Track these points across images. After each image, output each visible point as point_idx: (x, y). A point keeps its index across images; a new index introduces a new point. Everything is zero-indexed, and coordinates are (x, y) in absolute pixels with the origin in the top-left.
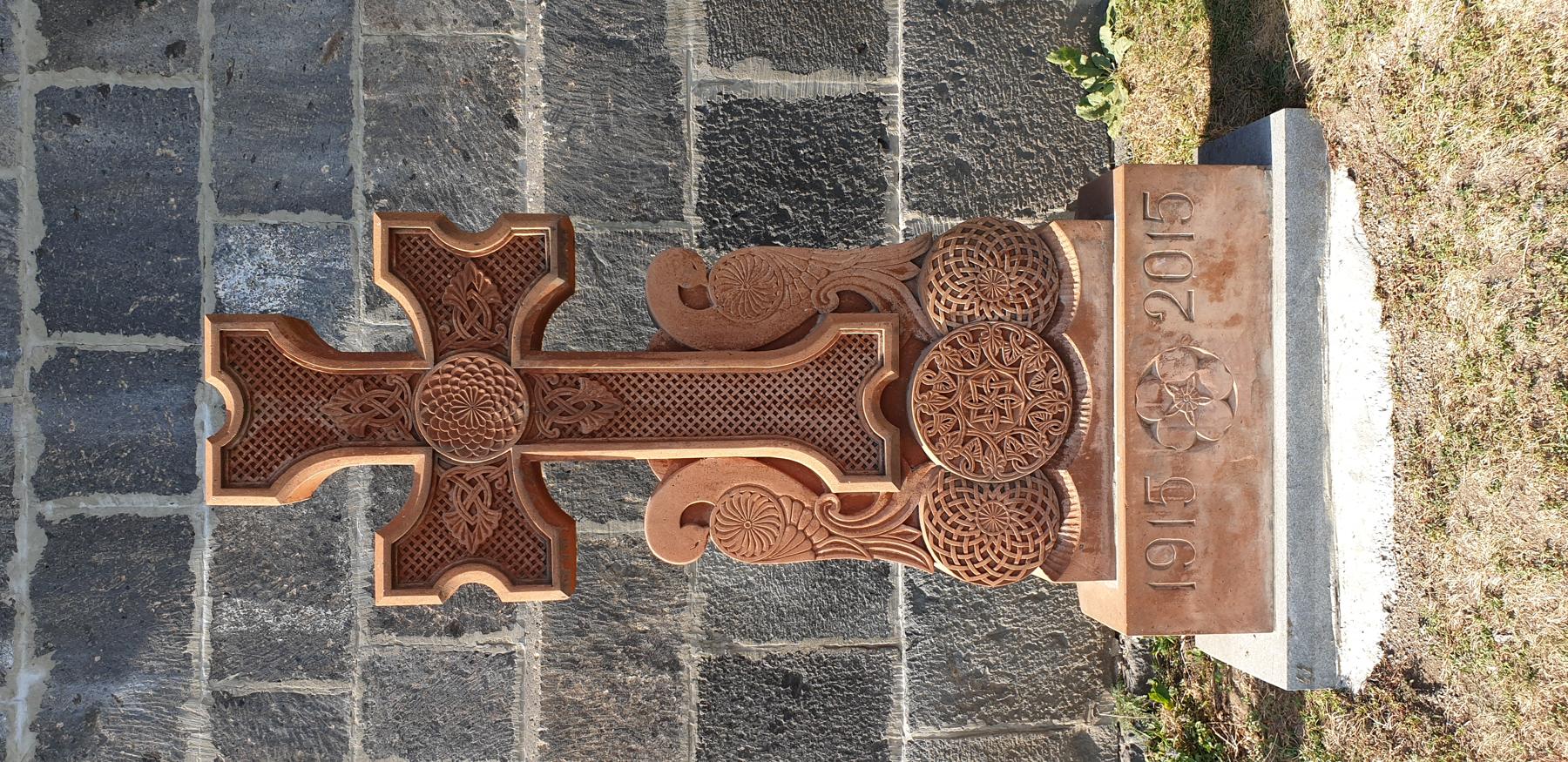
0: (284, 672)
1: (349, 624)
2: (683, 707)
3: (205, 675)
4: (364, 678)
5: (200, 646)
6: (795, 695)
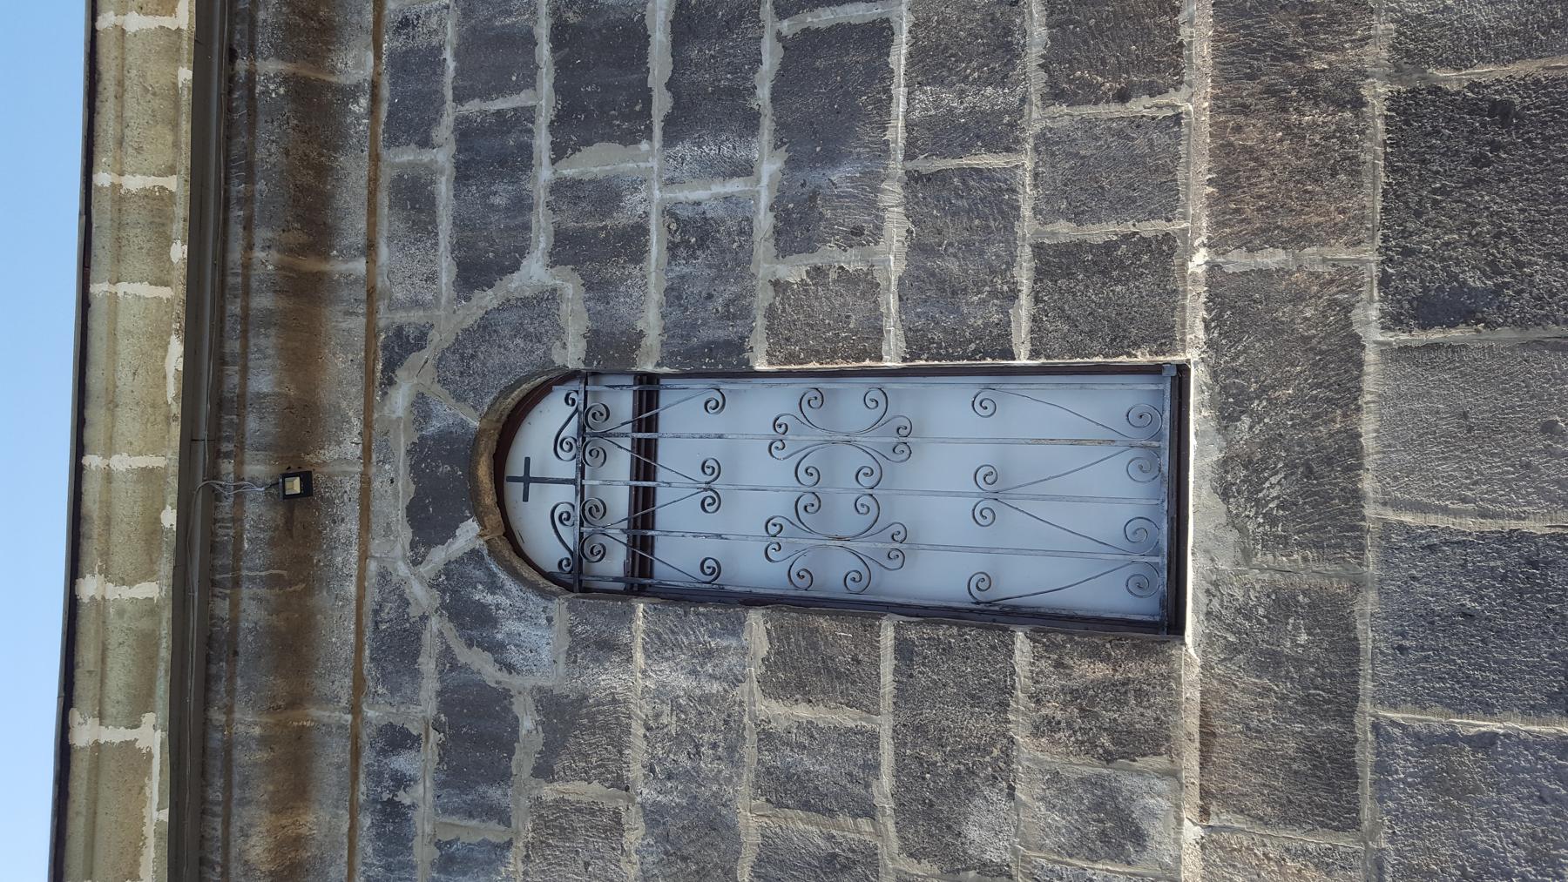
0: (966, 149)
1: (1023, 100)
2: (1368, 144)
3: (900, 157)
4: (1036, 149)
5: (897, 133)
6: (1505, 123)
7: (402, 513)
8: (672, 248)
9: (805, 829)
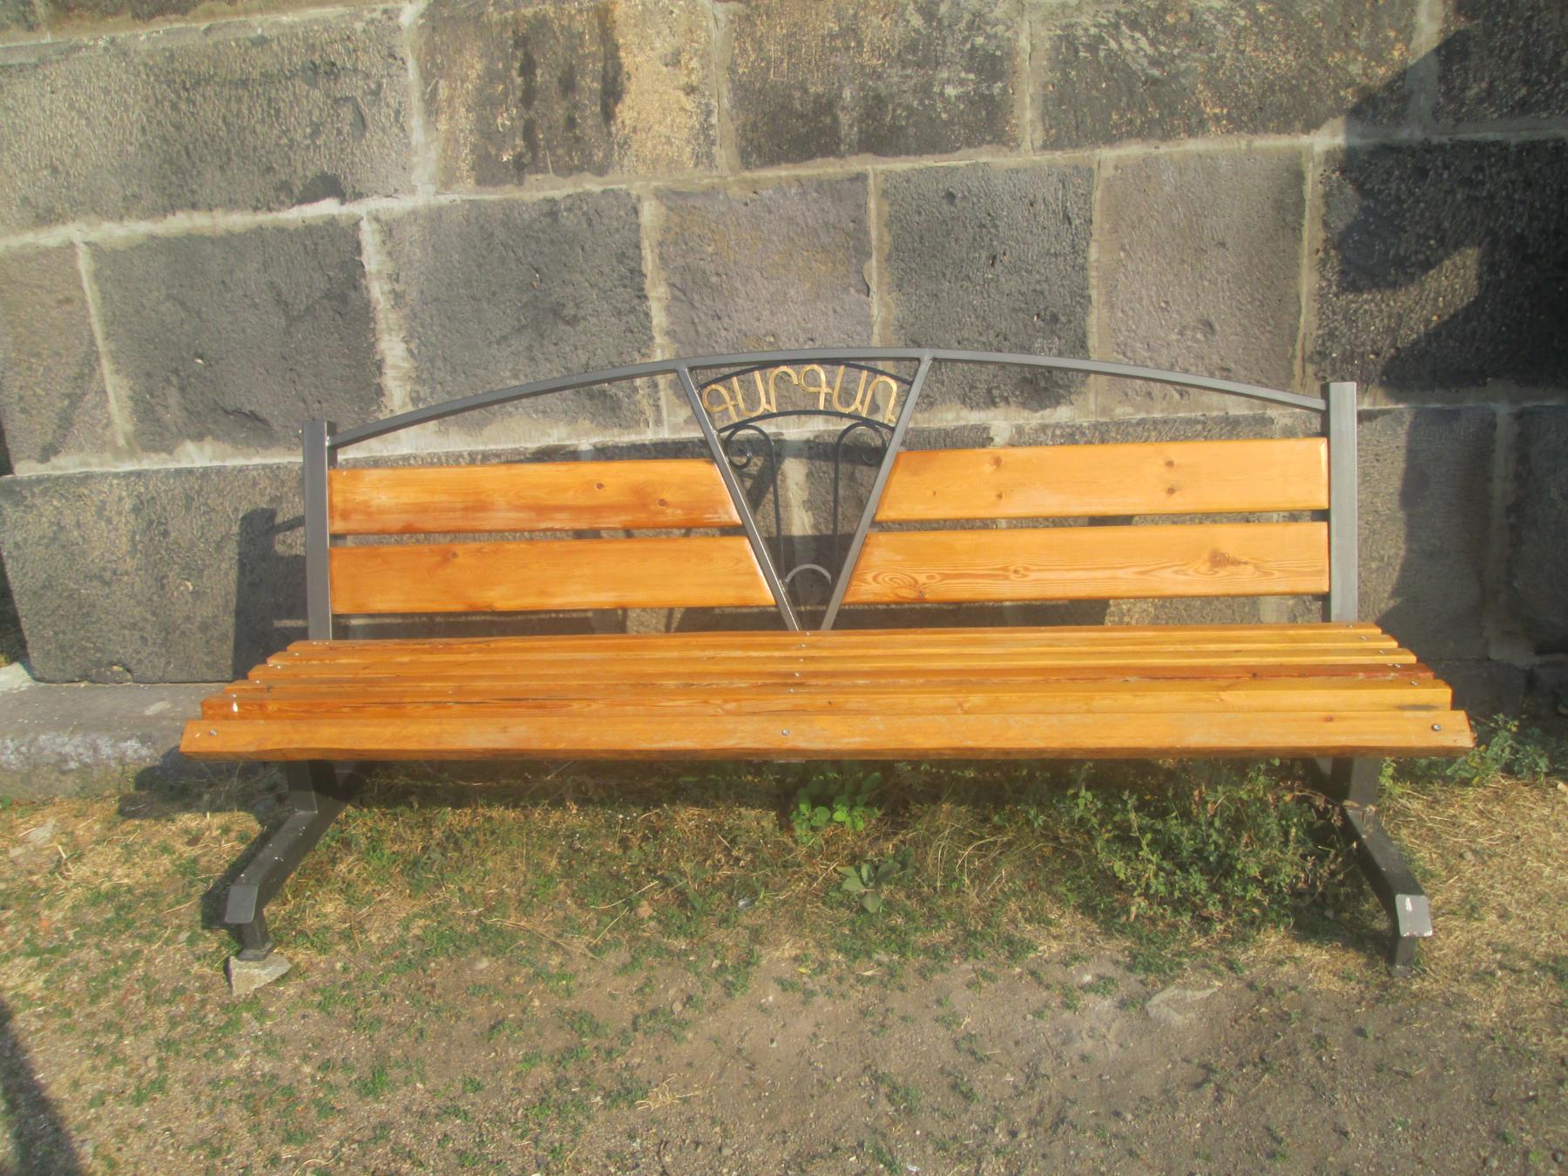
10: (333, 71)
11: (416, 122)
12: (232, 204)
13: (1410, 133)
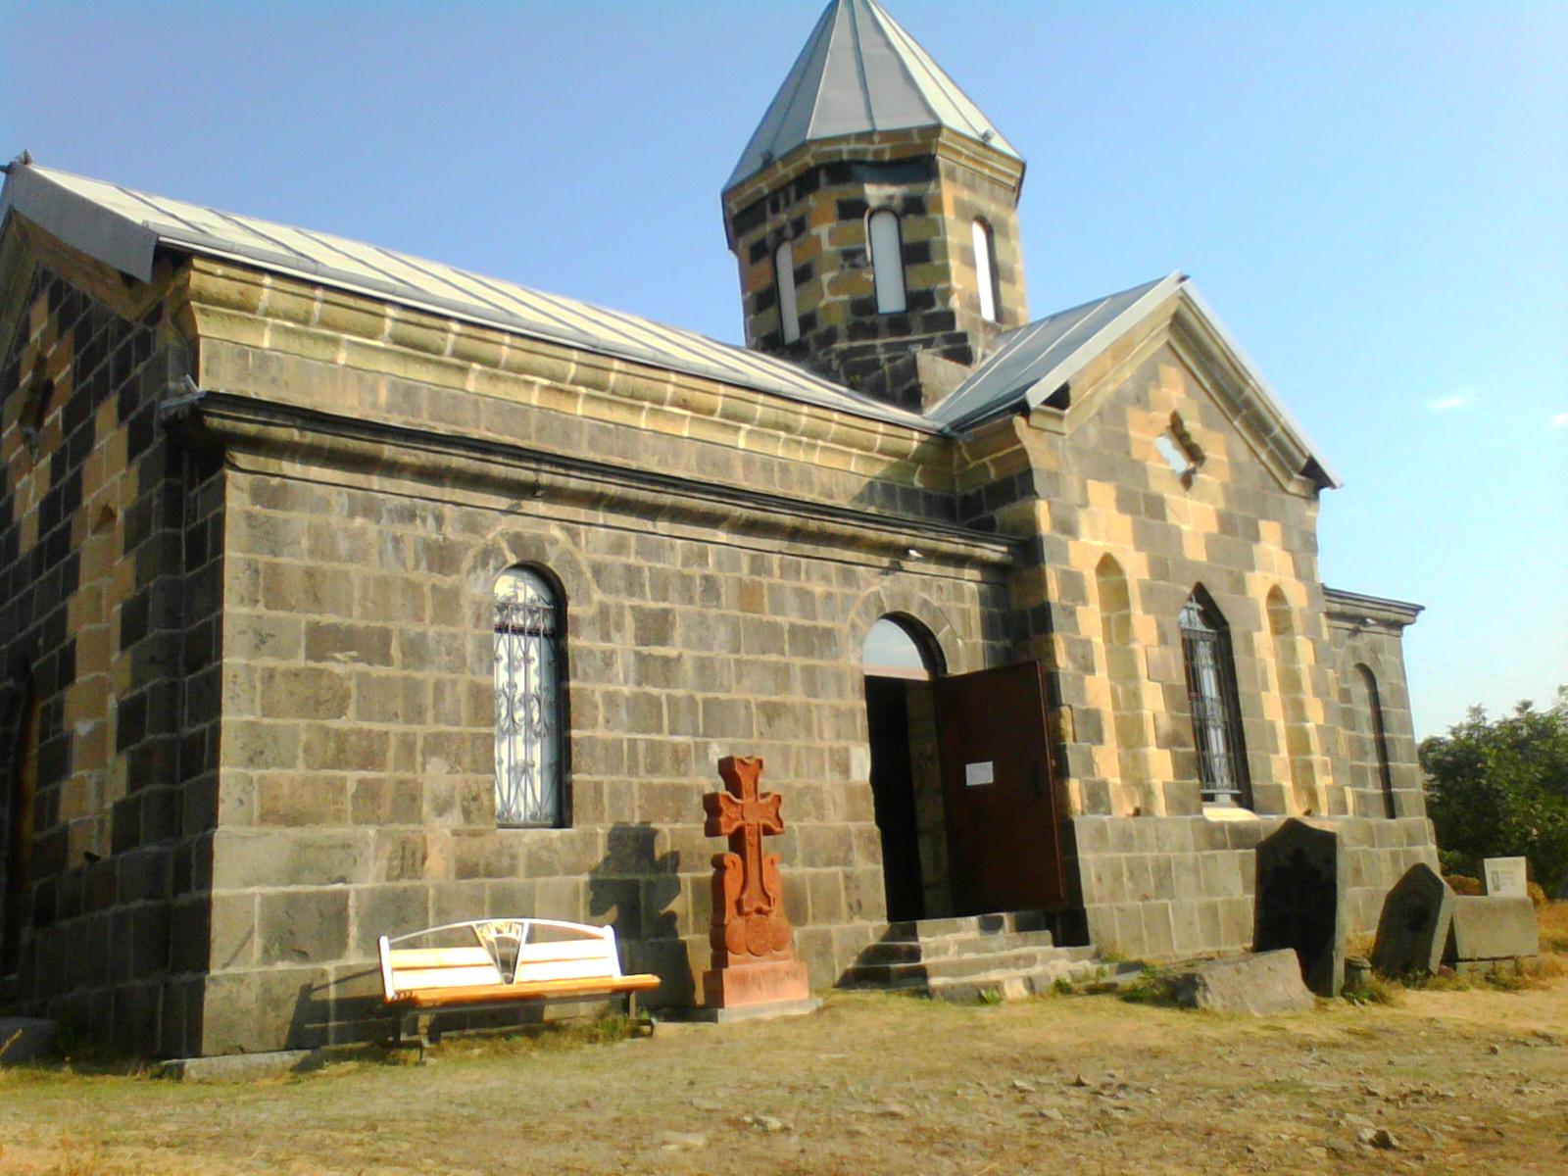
7: (519, 529)
8: (604, 652)
9: (428, 698)
10: (350, 846)
11: (371, 864)
12: (311, 883)
13: (599, 877)
